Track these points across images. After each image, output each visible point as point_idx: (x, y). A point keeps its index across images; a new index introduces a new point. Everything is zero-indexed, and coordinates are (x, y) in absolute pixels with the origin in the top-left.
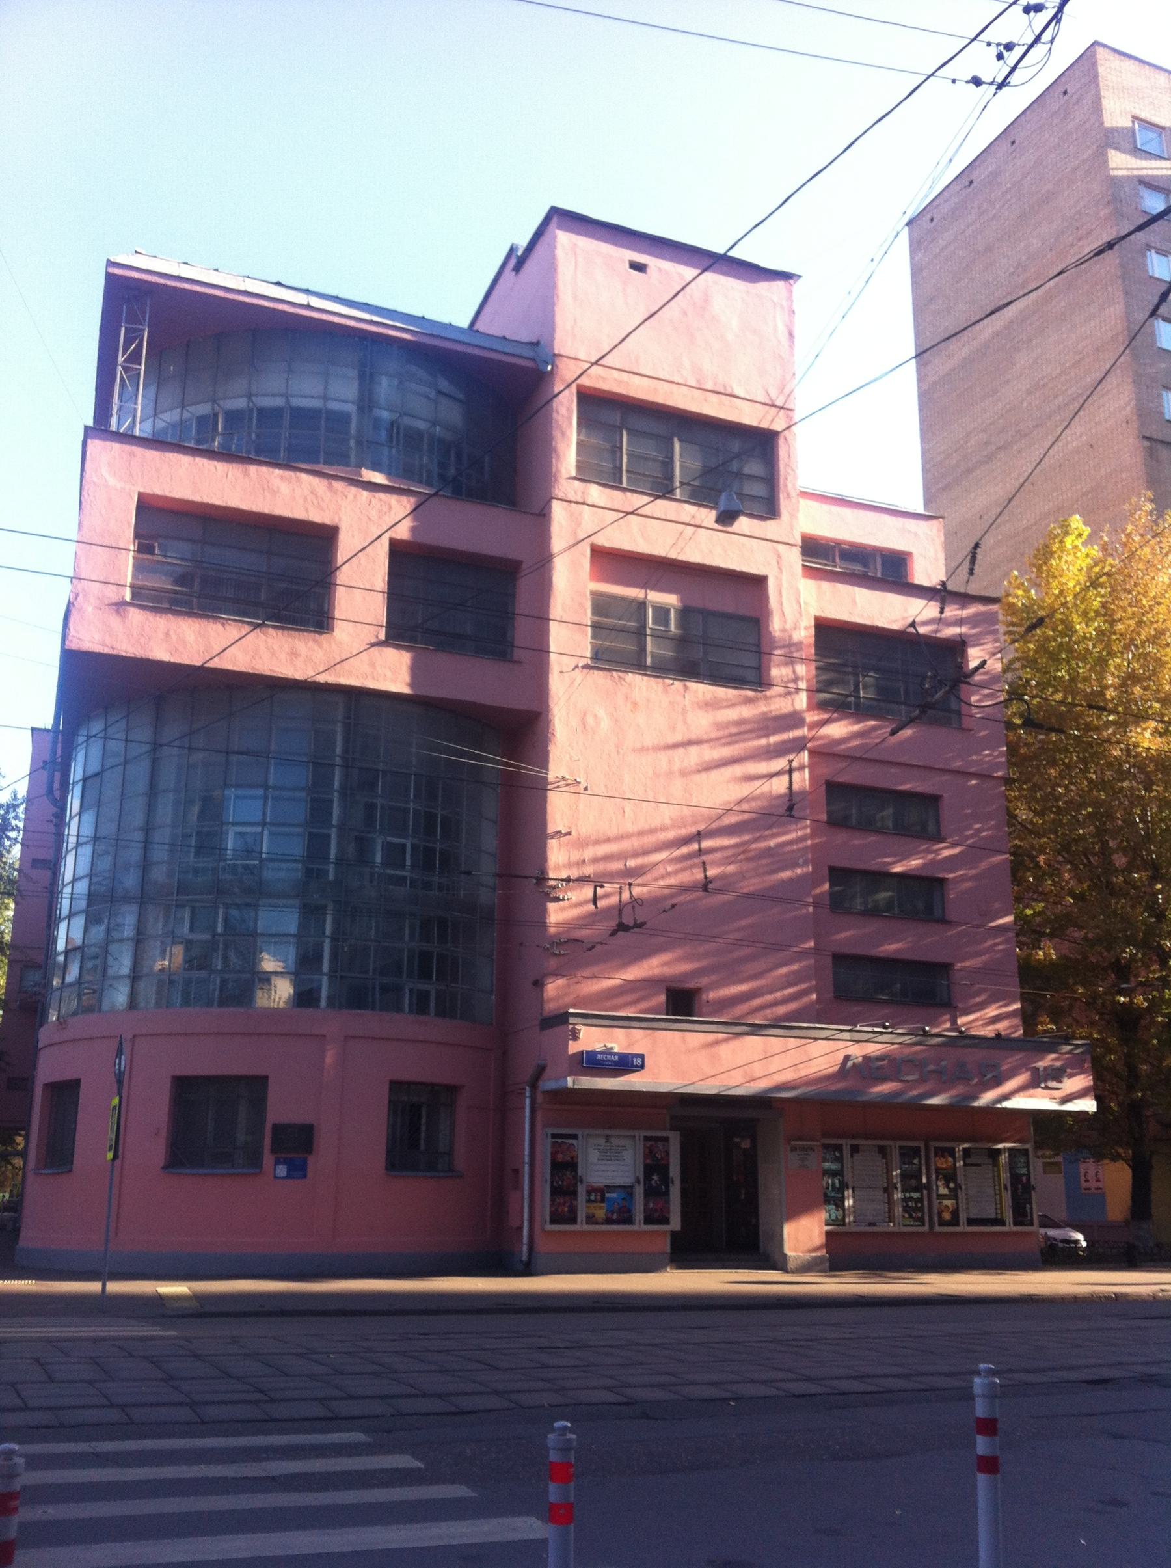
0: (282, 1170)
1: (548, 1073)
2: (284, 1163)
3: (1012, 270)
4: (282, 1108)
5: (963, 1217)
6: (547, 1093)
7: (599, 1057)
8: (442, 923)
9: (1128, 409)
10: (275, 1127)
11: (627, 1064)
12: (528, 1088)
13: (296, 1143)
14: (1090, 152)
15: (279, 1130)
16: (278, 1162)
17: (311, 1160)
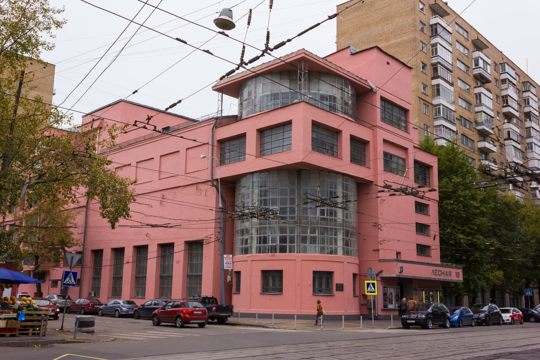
1: (384, 272)
4: (337, 280)
13: (340, 288)
15: (337, 284)
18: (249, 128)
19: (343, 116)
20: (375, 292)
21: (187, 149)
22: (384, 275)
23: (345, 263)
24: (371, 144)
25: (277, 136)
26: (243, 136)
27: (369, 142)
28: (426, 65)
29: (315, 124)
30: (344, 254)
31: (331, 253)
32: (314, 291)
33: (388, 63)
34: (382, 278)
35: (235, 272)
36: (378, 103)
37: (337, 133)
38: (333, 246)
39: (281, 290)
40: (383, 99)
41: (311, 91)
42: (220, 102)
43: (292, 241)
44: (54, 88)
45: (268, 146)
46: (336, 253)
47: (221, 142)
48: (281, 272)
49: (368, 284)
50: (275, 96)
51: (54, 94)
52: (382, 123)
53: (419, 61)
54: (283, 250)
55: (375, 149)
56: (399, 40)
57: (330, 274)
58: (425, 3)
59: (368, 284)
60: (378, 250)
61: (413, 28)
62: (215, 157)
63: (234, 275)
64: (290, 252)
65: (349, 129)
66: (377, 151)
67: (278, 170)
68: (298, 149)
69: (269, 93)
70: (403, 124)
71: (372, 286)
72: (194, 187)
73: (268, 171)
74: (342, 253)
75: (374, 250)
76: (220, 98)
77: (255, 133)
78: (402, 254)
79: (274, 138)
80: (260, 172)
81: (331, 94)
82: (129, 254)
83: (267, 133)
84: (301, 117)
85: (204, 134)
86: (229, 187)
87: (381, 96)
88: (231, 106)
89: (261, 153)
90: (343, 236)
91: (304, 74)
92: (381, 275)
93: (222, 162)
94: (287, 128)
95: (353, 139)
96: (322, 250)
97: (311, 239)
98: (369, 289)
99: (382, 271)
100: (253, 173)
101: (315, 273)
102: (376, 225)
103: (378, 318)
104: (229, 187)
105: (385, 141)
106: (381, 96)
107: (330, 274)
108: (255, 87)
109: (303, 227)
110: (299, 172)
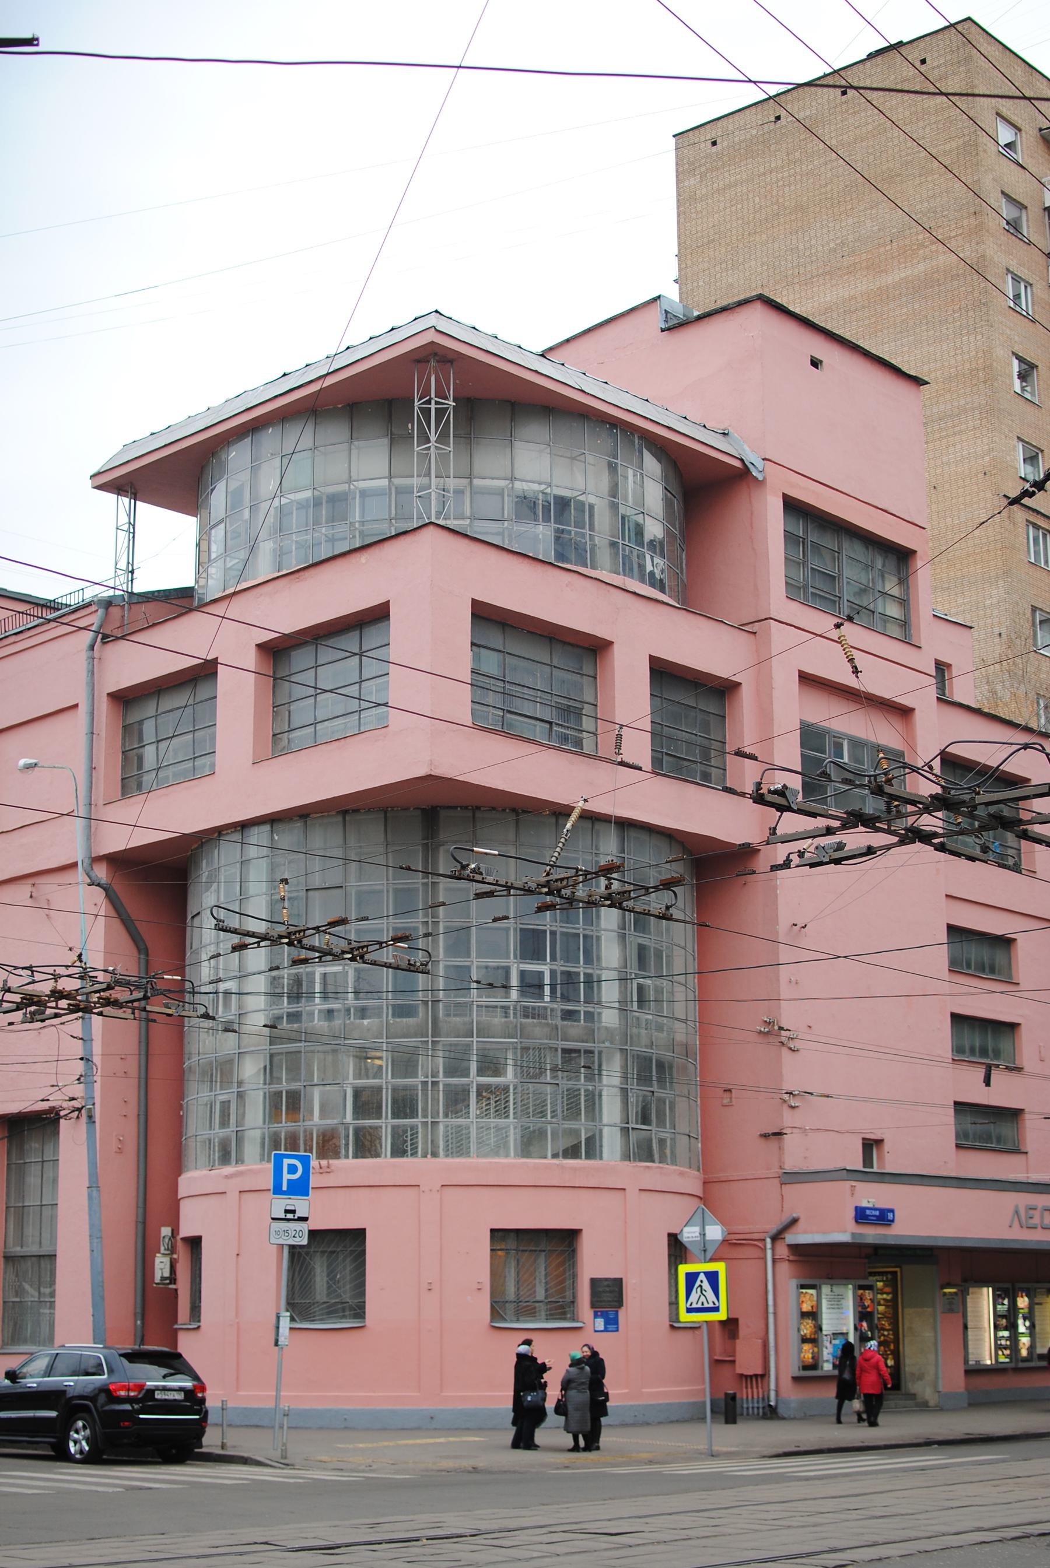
0: (600, 1324)
1: (801, 1225)
2: (602, 1316)
3: (832, 245)
4: (594, 1262)
5: (1035, 1356)
7: (868, 1212)
8: (661, 1065)
9: (987, 459)
10: (593, 1281)
11: (884, 1217)
12: (768, 1241)
14: (954, 144)
15: (593, 1281)
16: (596, 1316)
17: (622, 1313)
18: (231, 643)
19: (618, 580)
20: (716, 1309)
22: (801, 1236)
23: (632, 1193)
24: (747, 695)
25: (335, 669)
26: (205, 672)
27: (738, 685)
28: (1032, 366)
29: (486, 616)
30: (626, 1157)
31: (572, 1152)
33: (815, 363)
34: (795, 1248)
35: (184, 1239)
36: (774, 521)
37: (592, 649)
38: (583, 1127)
39: (359, 1312)
40: (792, 506)
41: (477, 482)
42: (123, 536)
43: (404, 1106)
45: (302, 713)
46: (593, 1148)
47: (126, 699)
48: (359, 1235)
49: (692, 1278)
50: (335, 505)
52: (794, 606)
53: (1001, 352)
54: (366, 1145)
55: (766, 715)
56: (921, 267)
57: (564, 1241)
58: (1019, 122)
59: (692, 1278)
60: (779, 1134)
61: (973, 221)
62: (100, 761)
63: (183, 1255)
64: (399, 1151)
65: (643, 632)
67: (344, 813)
68: (419, 721)
69: (308, 494)
70: (893, 610)
71: (706, 1285)
73: (302, 815)
74: (618, 1154)
75: (765, 1136)
76: (124, 519)
77: (250, 659)
78: (887, 1146)
79: (327, 677)
80: (273, 820)
81: (567, 493)
83: (301, 658)
84: (429, 591)
85: (61, 671)
86: (157, 882)
87: (785, 496)
88: (167, 548)
89: (278, 739)
90: (625, 1078)
91: (441, 413)
92: (791, 1238)
93: (132, 781)
94: (372, 637)
95: (664, 674)
96: (530, 1143)
97: (479, 1094)
98: (694, 1295)
99: (794, 1221)
100: (243, 826)
101: (497, 1235)
102: (773, 1032)
103: (781, 1411)
104: (157, 882)
105: (806, 679)
106: (785, 496)
107: (564, 1241)
108: (254, 470)
109: (450, 1048)
110: (427, 816)
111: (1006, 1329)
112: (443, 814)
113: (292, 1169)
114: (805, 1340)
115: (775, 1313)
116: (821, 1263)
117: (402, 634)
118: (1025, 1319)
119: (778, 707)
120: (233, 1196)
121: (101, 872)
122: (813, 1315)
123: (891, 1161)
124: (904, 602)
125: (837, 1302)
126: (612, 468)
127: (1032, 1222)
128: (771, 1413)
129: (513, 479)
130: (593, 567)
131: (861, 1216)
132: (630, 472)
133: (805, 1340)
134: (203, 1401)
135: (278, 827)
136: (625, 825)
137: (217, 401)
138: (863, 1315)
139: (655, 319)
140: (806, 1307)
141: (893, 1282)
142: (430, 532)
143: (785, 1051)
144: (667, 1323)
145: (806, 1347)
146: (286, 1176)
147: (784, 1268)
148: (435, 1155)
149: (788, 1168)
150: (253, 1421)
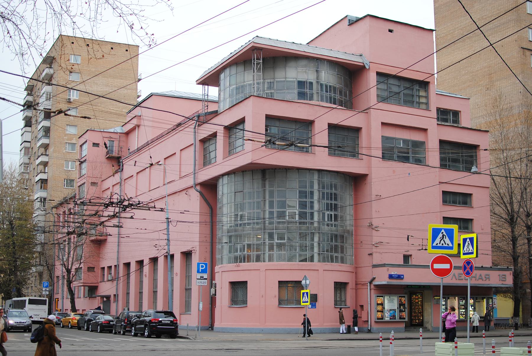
6: (375, 285)
11: (399, 277)
17: (317, 304)
21: (181, 150)
22: (376, 283)
30: (319, 261)
31: (305, 260)
32: (280, 303)
33: (391, 31)
34: (375, 286)
37: (309, 124)
44: (140, 71)
46: (312, 259)
47: (204, 141)
48: (246, 282)
51: (139, 80)
57: (298, 285)
59: (303, 293)
66: (373, 139)
67: (243, 172)
72: (185, 192)
78: (413, 257)
80: (228, 174)
82: (133, 267)
84: (254, 114)
91: (258, 64)
99: (374, 278)
101: (279, 281)
102: (371, 225)
111: (464, 309)
112: (267, 171)
113: (202, 266)
114: (378, 311)
115: (370, 304)
116: (384, 290)
117: (248, 125)
118: (472, 306)
119: (373, 134)
120: (221, 272)
121: (198, 188)
122: (382, 304)
123: (413, 261)
124: (427, 97)
125: (391, 301)
126: (317, 71)
127: (460, 278)
128: (369, 331)
129: (286, 78)
130: (310, 100)
131: (391, 277)
132: (323, 72)
133: (378, 311)
134: (177, 323)
135: (230, 176)
136: (320, 171)
137: (220, 61)
138: (401, 304)
139: (346, 22)
140: (379, 302)
141: (422, 296)
142: (252, 97)
143: (374, 231)
144: (334, 306)
145: (379, 313)
146: (201, 268)
147: (373, 291)
148: (264, 261)
149: (374, 264)
150: (188, 328)
